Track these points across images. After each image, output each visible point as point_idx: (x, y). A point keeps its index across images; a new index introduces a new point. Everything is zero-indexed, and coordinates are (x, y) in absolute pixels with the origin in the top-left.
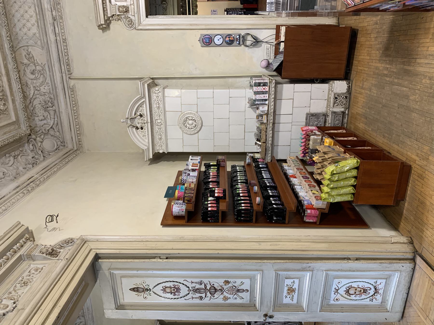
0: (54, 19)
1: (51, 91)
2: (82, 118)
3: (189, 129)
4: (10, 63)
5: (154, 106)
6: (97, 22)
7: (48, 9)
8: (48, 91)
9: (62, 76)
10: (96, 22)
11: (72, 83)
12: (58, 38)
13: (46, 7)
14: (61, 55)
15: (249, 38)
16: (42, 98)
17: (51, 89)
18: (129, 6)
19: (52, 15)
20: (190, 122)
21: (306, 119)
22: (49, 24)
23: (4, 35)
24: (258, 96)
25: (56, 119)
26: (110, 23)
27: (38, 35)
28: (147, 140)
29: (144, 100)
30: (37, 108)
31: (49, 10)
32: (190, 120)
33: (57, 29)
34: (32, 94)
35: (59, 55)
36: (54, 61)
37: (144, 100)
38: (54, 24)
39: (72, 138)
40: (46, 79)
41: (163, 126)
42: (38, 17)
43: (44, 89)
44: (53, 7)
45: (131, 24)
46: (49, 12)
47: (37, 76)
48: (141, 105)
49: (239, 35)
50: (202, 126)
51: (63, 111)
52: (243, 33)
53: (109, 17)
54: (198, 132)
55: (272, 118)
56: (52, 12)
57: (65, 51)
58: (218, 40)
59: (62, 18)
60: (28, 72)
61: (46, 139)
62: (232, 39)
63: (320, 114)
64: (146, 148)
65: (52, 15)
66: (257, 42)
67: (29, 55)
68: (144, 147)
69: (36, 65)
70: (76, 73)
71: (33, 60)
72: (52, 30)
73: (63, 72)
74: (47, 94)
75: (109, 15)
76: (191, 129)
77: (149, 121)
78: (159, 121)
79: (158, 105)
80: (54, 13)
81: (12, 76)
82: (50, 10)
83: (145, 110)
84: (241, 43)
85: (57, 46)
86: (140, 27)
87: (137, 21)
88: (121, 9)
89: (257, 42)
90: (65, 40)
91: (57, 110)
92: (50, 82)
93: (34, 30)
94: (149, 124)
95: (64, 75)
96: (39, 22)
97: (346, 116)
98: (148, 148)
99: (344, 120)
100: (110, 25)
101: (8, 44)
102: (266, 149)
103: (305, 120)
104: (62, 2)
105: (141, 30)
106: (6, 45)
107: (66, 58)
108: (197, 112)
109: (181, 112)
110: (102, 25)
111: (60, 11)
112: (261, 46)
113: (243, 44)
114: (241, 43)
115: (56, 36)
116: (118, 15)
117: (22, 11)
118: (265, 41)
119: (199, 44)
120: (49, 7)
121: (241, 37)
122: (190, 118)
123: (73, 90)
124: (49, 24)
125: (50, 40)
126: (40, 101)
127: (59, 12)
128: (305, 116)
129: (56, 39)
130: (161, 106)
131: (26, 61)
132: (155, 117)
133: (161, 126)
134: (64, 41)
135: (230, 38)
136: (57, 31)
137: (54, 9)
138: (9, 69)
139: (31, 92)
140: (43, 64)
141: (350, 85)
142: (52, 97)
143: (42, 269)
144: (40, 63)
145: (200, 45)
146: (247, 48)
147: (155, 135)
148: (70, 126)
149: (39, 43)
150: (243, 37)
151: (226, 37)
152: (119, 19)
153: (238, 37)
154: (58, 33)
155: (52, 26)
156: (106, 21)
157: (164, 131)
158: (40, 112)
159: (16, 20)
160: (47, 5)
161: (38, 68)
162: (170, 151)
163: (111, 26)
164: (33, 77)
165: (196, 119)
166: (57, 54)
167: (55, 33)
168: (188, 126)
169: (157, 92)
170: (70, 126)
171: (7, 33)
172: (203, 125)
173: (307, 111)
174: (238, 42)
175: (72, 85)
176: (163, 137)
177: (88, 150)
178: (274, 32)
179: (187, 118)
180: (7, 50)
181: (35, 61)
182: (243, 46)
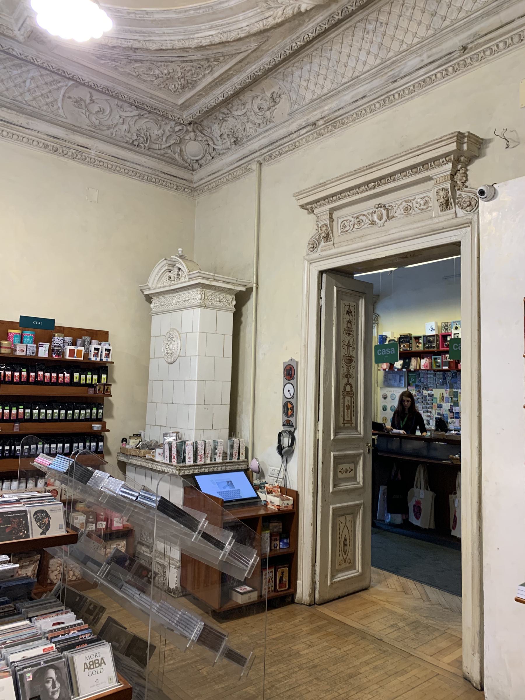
4: (238, 78)
7: (323, 112)
8: (248, 134)
9: (256, 152)
10: (297, 193)
11: (254, 166)
12: (295, 136)
13: (326, 108)
17: (251, 137)
18: (332, 242)
19: (318, 120)
22: (306, 118)
23: (264, 60)
24: (191, 448)
27: (304, 103)
33: (304, 131)
35: (277, 141)
36: (270, 136)
38: (308, 125)
39: (202, 179)
43: (250, 128)
44: (327, 120)
47: (260, 114)
51: (224, 161)
56: (321, 118)
58: (289, 391)
59: (319, 135)
64: (150, 285)
65: (318, 120)
69: (271, 110)
71: (272, 104)
72: (301, 125)
73: (261, 151)
77: (172, 288)
79: (187, 299)
80: (321, 122)
81: (227, 86)
82: (323, 115)
85: (286, 137)
90: (295, 147)
92: (257, 133)
93: (309, 96)
94: (168, 288)
95: (258, 154)
96: (318, 101)
101: (256, 70)
106: (254, 67)
111: (326, 130)
115: (295, 132)
119: (287, 359)
120: (326, 113)
124: (306, 118)
125: (290, 125)
126: (236, 126)
127: (324, 129)
129: (292, 134)
131: (269, 95)
135: (290, 411)
137: (325, 121)
138: (231, 80)
139: (238, 111)
140: (273, 120)
148: (212, 174)
149: (296, 107)
160: (327, 110)
166: (277, 138)
167: (299, 130)
170: (212, 174)
171: (267, 64)
177: (198, 203)
180: (250, 70)
181: (274, 108)
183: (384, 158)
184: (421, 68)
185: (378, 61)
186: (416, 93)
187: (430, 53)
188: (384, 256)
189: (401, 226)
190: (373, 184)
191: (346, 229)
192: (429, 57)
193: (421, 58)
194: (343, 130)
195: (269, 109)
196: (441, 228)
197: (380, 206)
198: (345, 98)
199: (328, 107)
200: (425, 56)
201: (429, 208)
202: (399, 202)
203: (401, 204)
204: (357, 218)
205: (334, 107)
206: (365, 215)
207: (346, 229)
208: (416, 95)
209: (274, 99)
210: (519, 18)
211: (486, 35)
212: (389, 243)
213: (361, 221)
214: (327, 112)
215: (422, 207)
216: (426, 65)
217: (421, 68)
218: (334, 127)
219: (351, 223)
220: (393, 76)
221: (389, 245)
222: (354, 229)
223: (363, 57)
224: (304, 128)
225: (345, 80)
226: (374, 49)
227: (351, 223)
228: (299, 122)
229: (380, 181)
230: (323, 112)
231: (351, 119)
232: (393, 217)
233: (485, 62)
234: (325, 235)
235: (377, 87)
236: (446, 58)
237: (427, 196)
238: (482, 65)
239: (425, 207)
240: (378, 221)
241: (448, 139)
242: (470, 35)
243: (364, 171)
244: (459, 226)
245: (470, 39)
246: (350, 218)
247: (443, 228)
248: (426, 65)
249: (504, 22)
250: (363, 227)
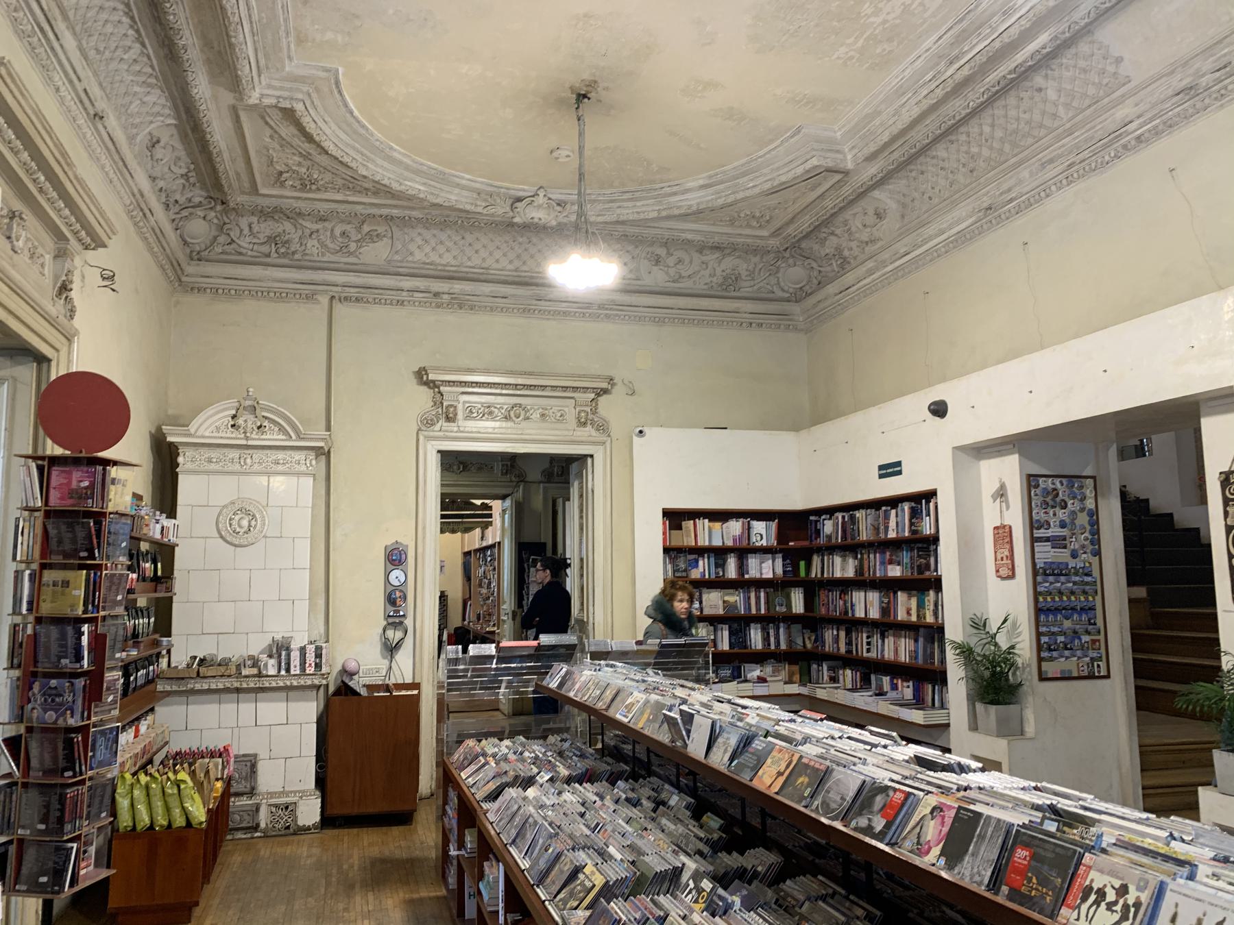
0: (436, 295)
1: (307, 258)
2: (250, 305)
3: (230, 520)
5: (280, 455)
8: (307, 252)
11: (325, 300)
12: (405, 294)
14: (376, 291)
15: (399, 635)
16: (295, 236)
17: (312, 258)
20: (245, 523)
21: (244, 756)
25: (250, 253)
26: (430, 388)
28: (207, 434)
29: (294, 437)
30: (276, 225)
32: (250, 522)
34: (304, 223)
37: (294, 437)
40: (332, 254)
41: (237, 467)
42: (440, 268)
45: (428, 423)
48: (282, 429)
49: (404, 616)
50: (236, 546)
52: (408, 622)
53: (439, 388)
54: (222, 537)
55: (252, 685)
57: (383, 301)
60: (348, 228)
61: (210, 227)
62: (398, 604)
63: (256, 781)
64: (192, 431)
66: (391, 649)
67: (378, 236)
68: (195, 427)
70: (340, 310)
74: (303, 247)
75: (441, 388)
76: (231, 525)
77: (250, 443)
78: (249, 461)
80: (446, 296)
83: (271, 437)
84: (391, 620)
86: (421, 438)
87: (431, 434)
88: (452, 409)
89: (391, 649)
90: (401, 303)
91: (268, 260)
92: (325, 259)
93: (419, 256)
94: (244, 442)
95: (339, 289)
97: (249, 835)
98: (190, 435)
99: (240, 833)
102: (183, 679)
103: (242, 753)
105: (418, 440)
107: (370, 300)
108: (265, 537)
109: (265, 504)
110: (427, 375)
112: (384, 658)
113: (389, 624)
114: (391, 620)
116: (442, 403)
117: (450, 244)
118: (393, 664)
120: (456, 291)
121: (402, 619)
122: (253, 523)
123: (310, 297)
128: (251, 752)
130: (280, 468)
132: (257, 455)
133: (238, 465)
136: (416, 294)
140: (360, 256)
141: (313, 831)
142: (296, 256)
143: (44, 275)
144: (362, 250)
145: (389, 543)
146: (381, 631)
147: (218, 450)
149: (397, 257)
150: (401, 623)
151: (401, 591)
152: (435, 404)
153: (402, 613)
156: (433, 382)
157: (226, 469)
158: (266, 228)
159: (435, 232)
161: (353, 246)
162: (180, 477)
163: (424, 388)
164: (337, 232)
165: (250, 534)
168: (237, 518)
169: (308, 462)
172: (238, 549)
173: (263, 754)
174: (391, 614)
175: (319, 297)
176: (213, 467)
177: (177, 303)
178: (409, 680)
179: (254, 516)
182: (385, 623)
185: (511, 267)
188: (522, 451)
195: (358, 241)
197: (520, 405)
198: (483, 288)
199: (458, 287)
209: (373, 237)
223: (498, 254)
225: (469, 264)
226: (511, 255)
232: (528, 418)
244: (594, 443)
246: (479, 406)
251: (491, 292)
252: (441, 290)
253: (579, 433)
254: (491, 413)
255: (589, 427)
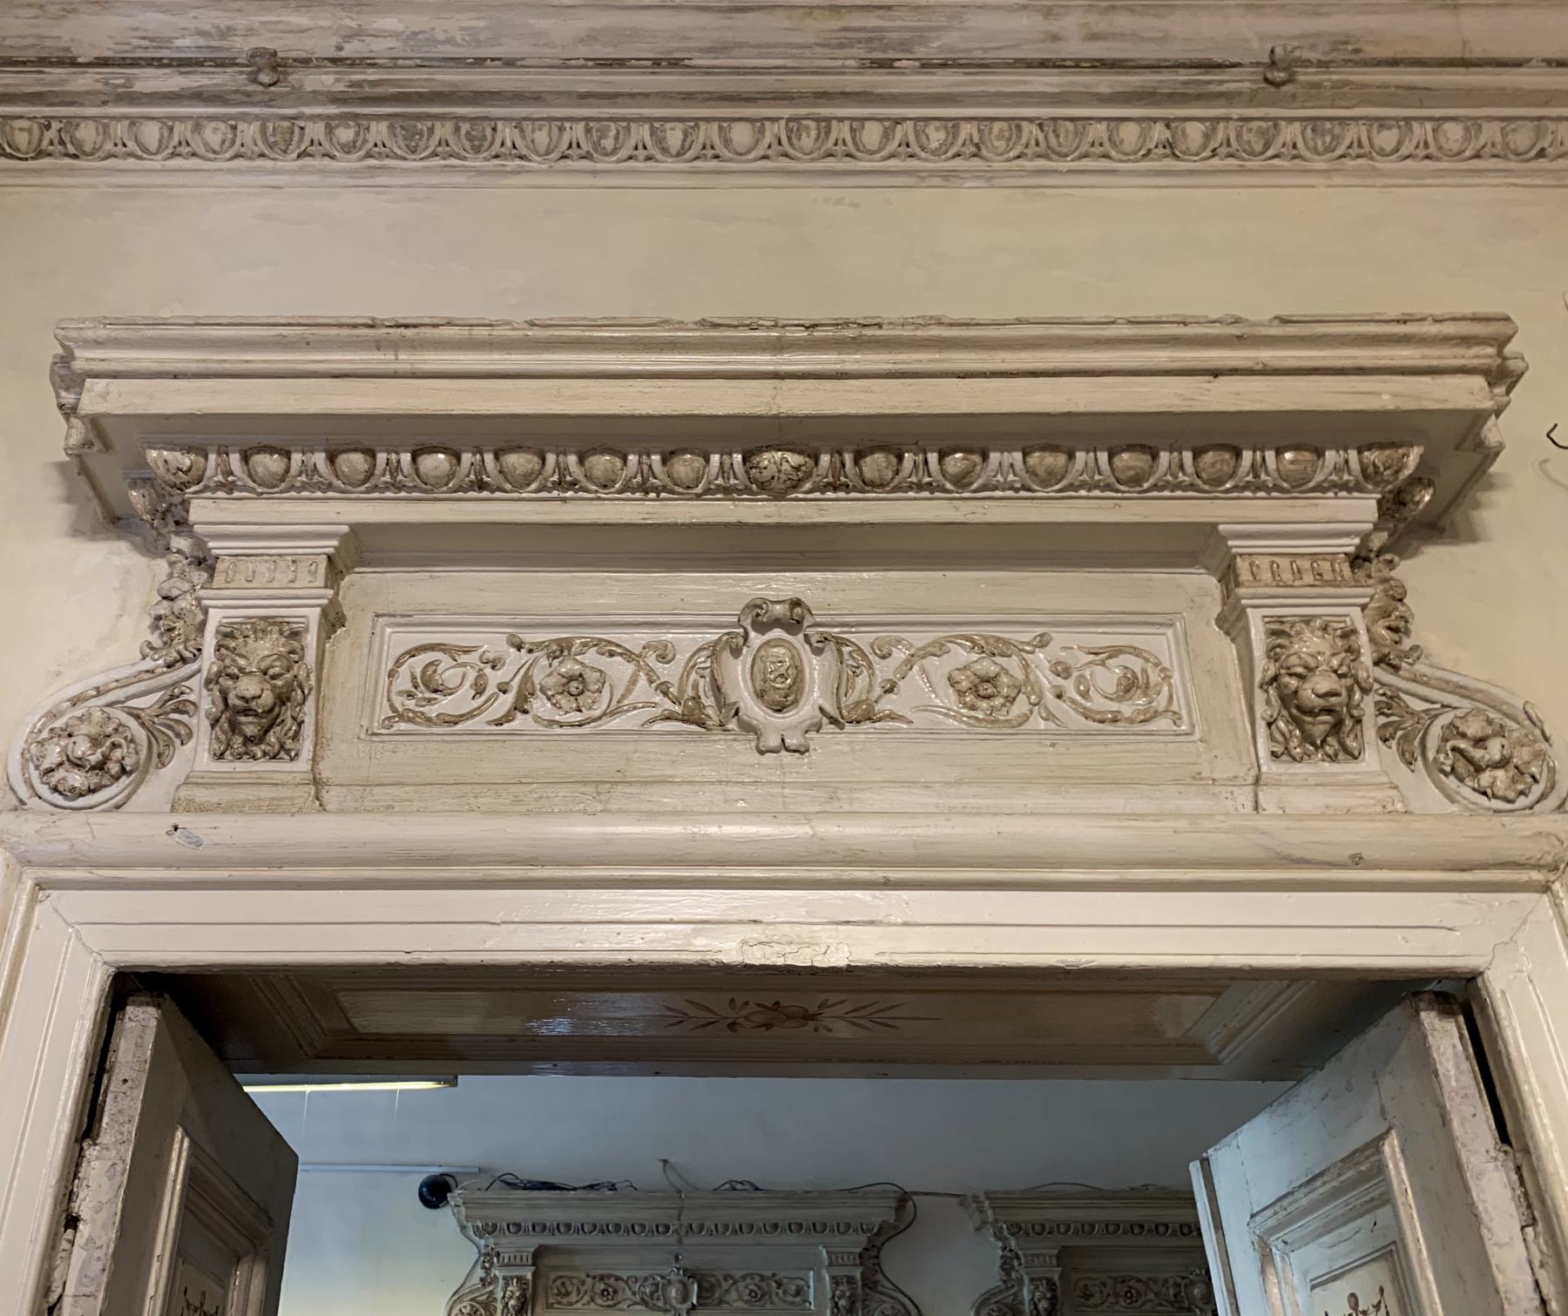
6: (102, 333)
7: (357, 34)
12: (85, 81)
13: (390, 23)
31: (349, 37)
33: (174, 81)
38: (221, 63)
46: (334, 40)
65: (305, 62)
75: (202, 511)
80: (327, 80)
82: (352, 49)
100: (123, 546)
104: (426, 170)
120: (380, 47)
129: (73, 63)
134: (52, 134)
154: (138, 87)
155: (201, 42)
160: (395, 35)
167: (134, 63)
183: (956, 315)
184: (1043, 64)
186: (976, 163)
187: (1100, 23)
188: (838, 959)
189: (958, 783)
190: (794, 459)
191: (445, 705)
192: (1093, 37)
193: (1053, 26)
194: (460, 179)
196: (1344, 854)
197: (794, 618)
200: (1070, 24)
201: (1163, 724)
202: (920, 638)
203: (938, 649)
204: (561, 650)
205: (450, 41)
206: (628, 655)
207: (445, 705)
208: (976, 174)
210: (1549, 62)
211: (1394, 63)
212: (895, 874)
213: (591, 676)
214: (392, 43)
215: (1098, 703)
216: (1077, 64)
217: (1043, 64)
218: (411, 134)
219: (494, 678)
220: (873, 37)
221: (887, 885)
222: (520, 721)
224: (183, 64)
227: (494, 678)
228: (153, 21)
229: (859, 457)
230: (357, 34)
231: (541, 138)
233: (1357, 172)
234: (268, 698)
235: (762, 48)
236: (1183, 76)
237: (1136, 652)
238: (1337, 180)
239: (1126, 709)
240: (754, 710)
241: (1446, 340)
242: (1318, 35)
243: (779, 346)
245: (1313, 47)
246: (492, 642)
247: (1357, 861)
248: (1077, 64)
249: (1477, 52)
250: (615, 723)
251: (592, 37)
252: (287, 46)
253: (1304, 800)
254: (575, 686)
255: (1376, 758)
